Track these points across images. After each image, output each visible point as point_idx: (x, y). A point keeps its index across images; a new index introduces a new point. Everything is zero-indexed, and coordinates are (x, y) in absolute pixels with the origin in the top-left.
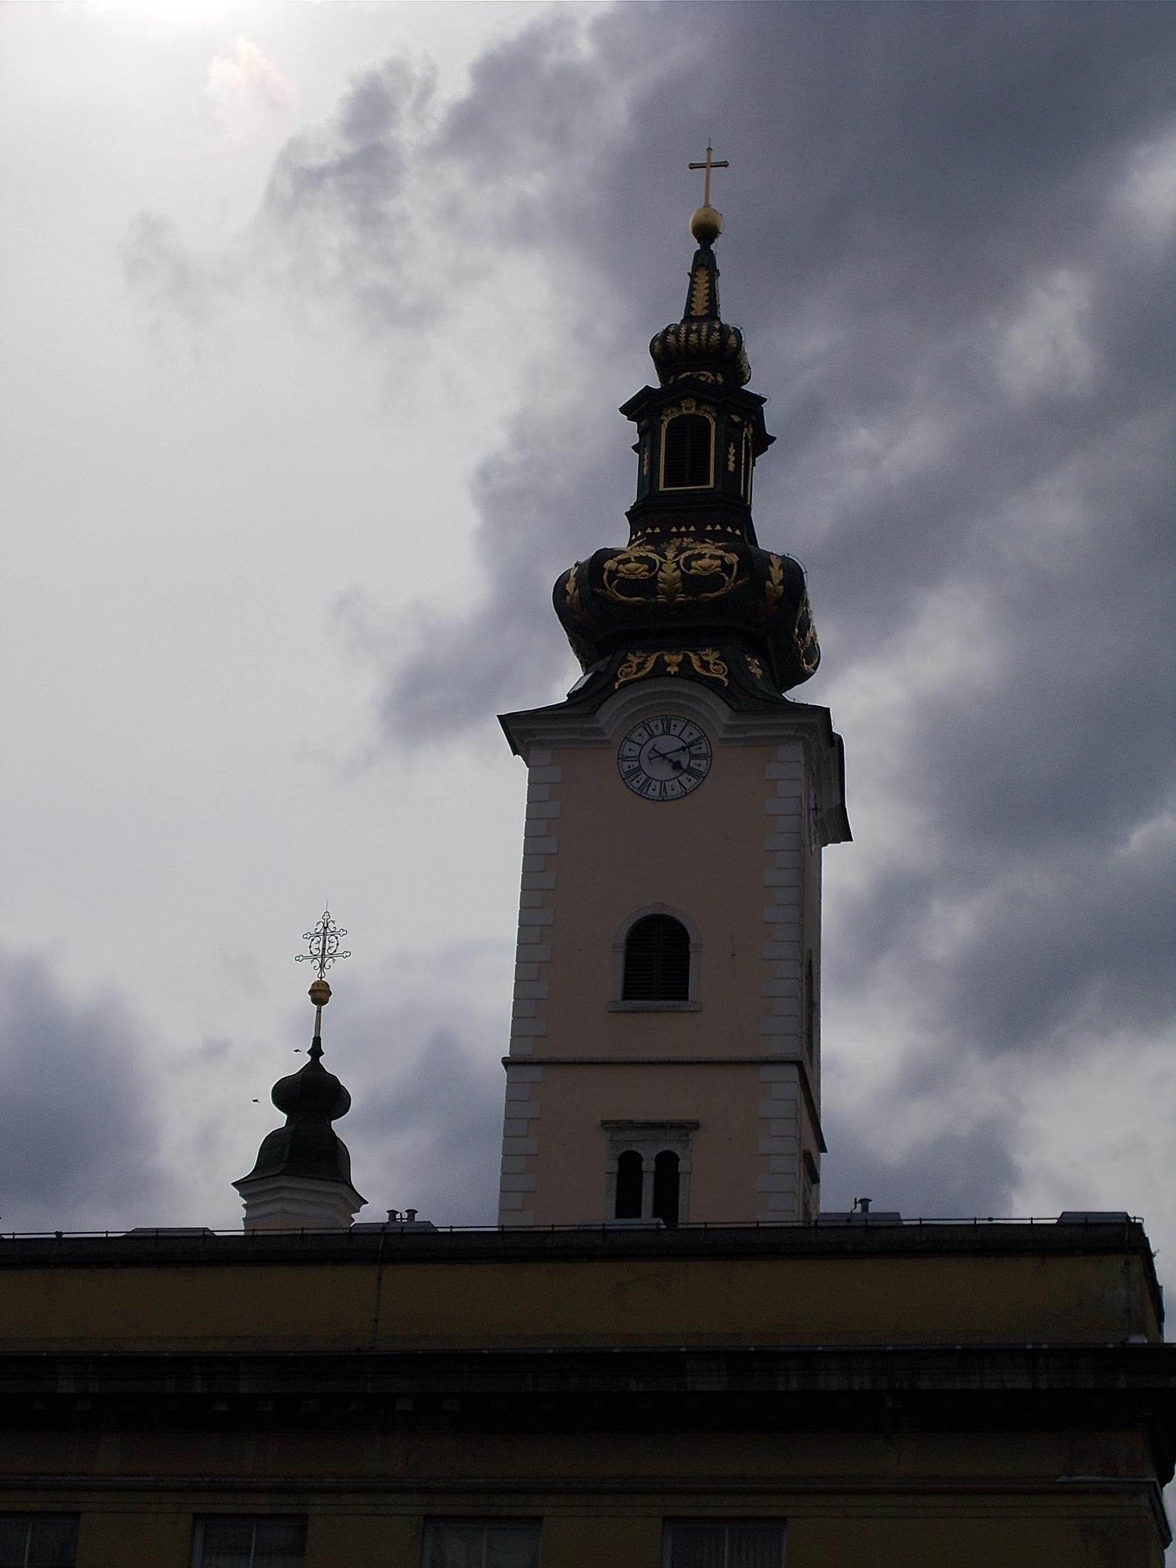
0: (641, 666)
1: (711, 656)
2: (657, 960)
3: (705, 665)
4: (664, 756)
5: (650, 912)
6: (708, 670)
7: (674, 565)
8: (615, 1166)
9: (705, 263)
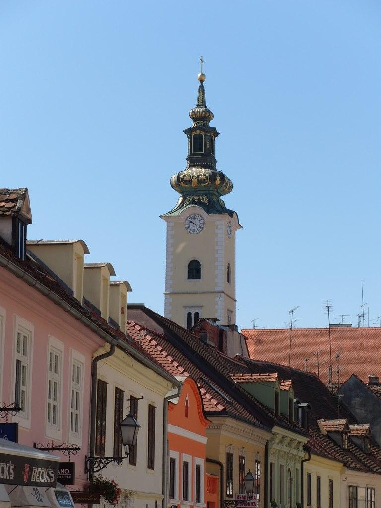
0: (189, 200)
1: (205, 198)
2: (194, 270)
3: (203, 200)
5: (193, 260)
8: (186, 315)
9: (202, 88)
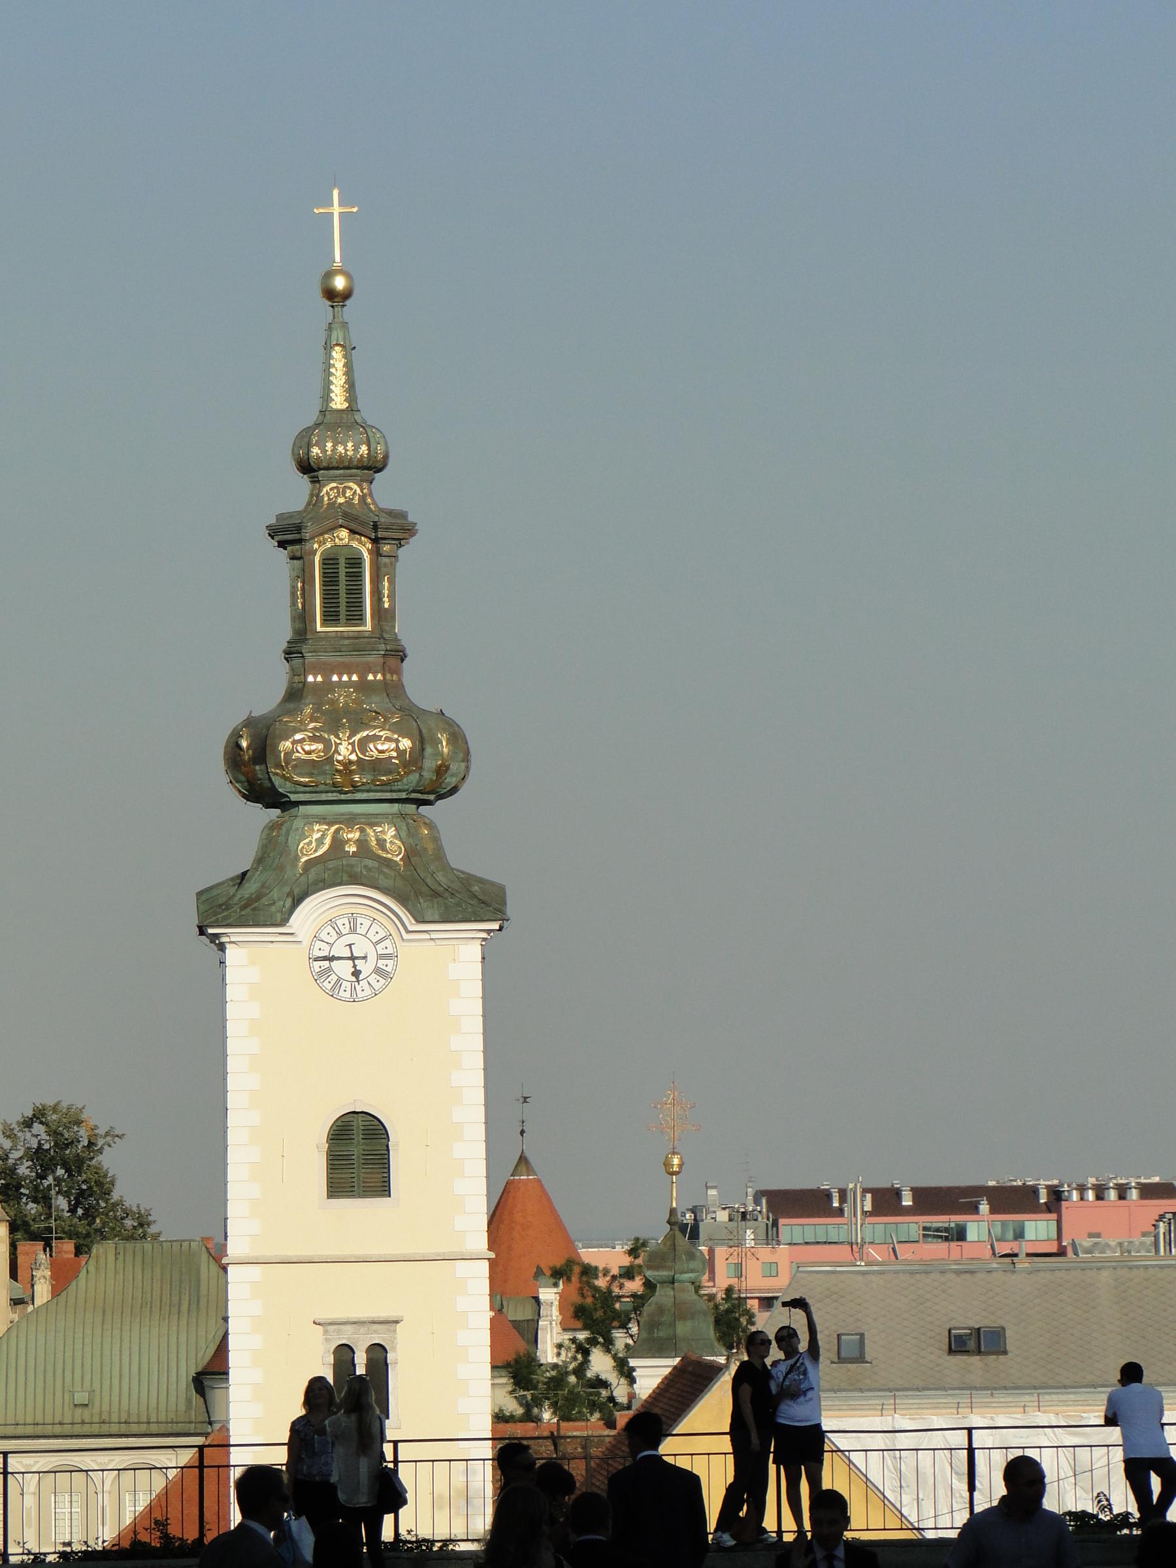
3: (381, 843)
4: (353, 958)
6: (384, 849)
7: (350, 747)
